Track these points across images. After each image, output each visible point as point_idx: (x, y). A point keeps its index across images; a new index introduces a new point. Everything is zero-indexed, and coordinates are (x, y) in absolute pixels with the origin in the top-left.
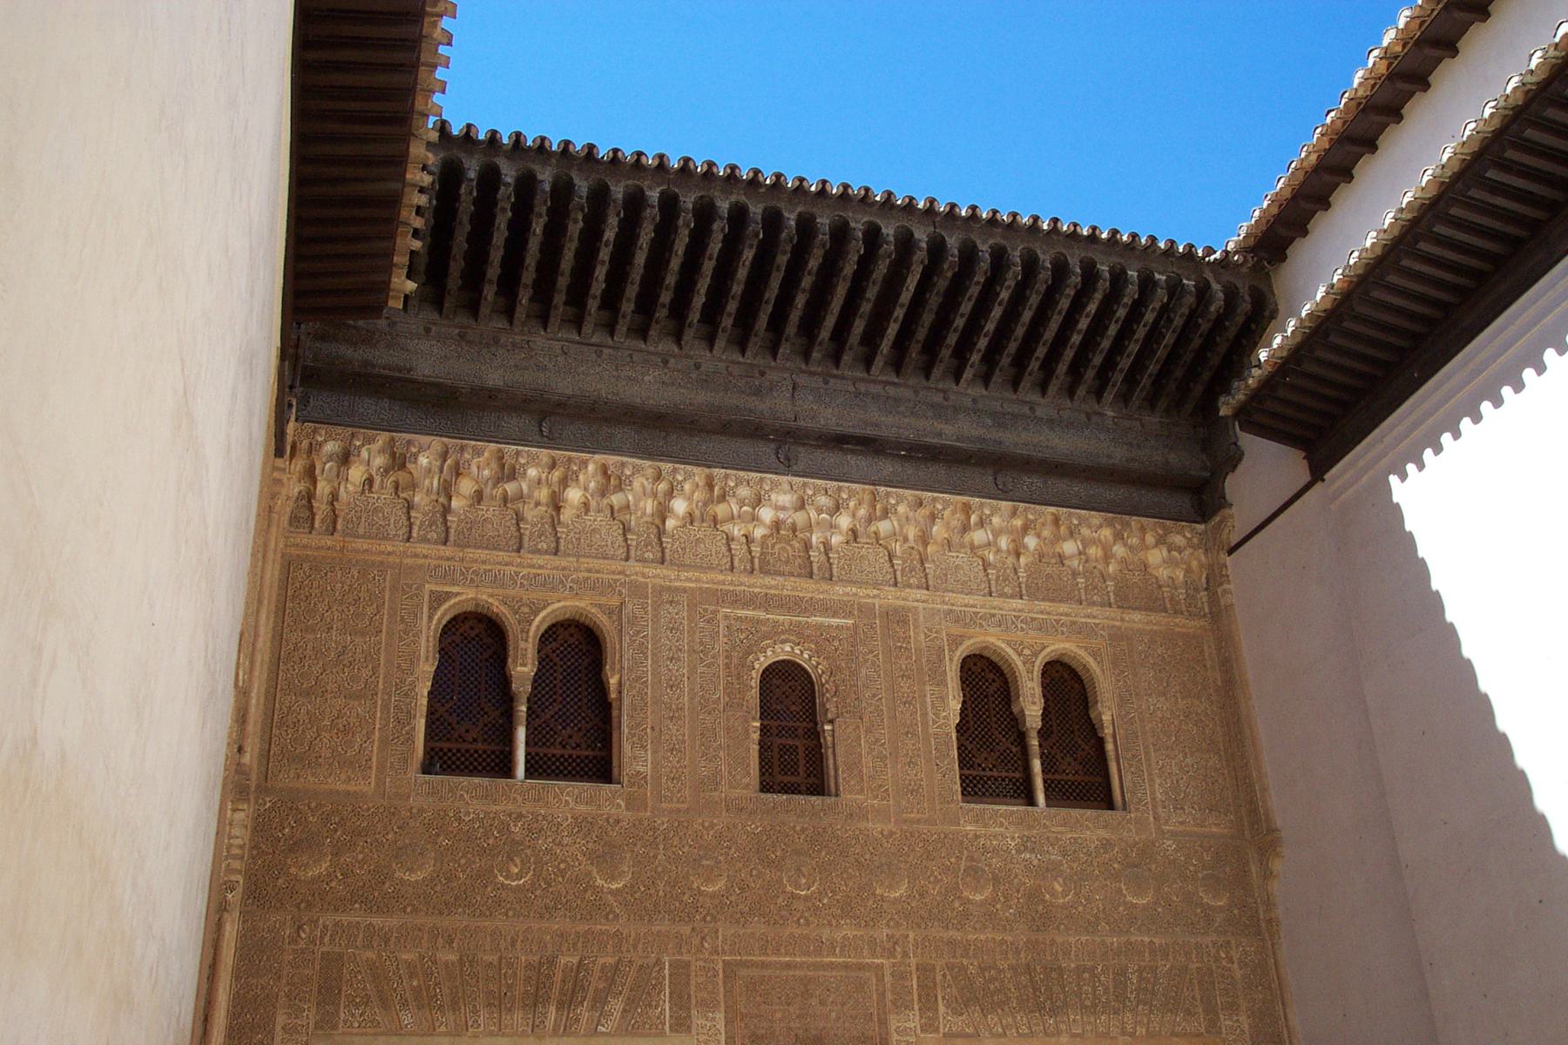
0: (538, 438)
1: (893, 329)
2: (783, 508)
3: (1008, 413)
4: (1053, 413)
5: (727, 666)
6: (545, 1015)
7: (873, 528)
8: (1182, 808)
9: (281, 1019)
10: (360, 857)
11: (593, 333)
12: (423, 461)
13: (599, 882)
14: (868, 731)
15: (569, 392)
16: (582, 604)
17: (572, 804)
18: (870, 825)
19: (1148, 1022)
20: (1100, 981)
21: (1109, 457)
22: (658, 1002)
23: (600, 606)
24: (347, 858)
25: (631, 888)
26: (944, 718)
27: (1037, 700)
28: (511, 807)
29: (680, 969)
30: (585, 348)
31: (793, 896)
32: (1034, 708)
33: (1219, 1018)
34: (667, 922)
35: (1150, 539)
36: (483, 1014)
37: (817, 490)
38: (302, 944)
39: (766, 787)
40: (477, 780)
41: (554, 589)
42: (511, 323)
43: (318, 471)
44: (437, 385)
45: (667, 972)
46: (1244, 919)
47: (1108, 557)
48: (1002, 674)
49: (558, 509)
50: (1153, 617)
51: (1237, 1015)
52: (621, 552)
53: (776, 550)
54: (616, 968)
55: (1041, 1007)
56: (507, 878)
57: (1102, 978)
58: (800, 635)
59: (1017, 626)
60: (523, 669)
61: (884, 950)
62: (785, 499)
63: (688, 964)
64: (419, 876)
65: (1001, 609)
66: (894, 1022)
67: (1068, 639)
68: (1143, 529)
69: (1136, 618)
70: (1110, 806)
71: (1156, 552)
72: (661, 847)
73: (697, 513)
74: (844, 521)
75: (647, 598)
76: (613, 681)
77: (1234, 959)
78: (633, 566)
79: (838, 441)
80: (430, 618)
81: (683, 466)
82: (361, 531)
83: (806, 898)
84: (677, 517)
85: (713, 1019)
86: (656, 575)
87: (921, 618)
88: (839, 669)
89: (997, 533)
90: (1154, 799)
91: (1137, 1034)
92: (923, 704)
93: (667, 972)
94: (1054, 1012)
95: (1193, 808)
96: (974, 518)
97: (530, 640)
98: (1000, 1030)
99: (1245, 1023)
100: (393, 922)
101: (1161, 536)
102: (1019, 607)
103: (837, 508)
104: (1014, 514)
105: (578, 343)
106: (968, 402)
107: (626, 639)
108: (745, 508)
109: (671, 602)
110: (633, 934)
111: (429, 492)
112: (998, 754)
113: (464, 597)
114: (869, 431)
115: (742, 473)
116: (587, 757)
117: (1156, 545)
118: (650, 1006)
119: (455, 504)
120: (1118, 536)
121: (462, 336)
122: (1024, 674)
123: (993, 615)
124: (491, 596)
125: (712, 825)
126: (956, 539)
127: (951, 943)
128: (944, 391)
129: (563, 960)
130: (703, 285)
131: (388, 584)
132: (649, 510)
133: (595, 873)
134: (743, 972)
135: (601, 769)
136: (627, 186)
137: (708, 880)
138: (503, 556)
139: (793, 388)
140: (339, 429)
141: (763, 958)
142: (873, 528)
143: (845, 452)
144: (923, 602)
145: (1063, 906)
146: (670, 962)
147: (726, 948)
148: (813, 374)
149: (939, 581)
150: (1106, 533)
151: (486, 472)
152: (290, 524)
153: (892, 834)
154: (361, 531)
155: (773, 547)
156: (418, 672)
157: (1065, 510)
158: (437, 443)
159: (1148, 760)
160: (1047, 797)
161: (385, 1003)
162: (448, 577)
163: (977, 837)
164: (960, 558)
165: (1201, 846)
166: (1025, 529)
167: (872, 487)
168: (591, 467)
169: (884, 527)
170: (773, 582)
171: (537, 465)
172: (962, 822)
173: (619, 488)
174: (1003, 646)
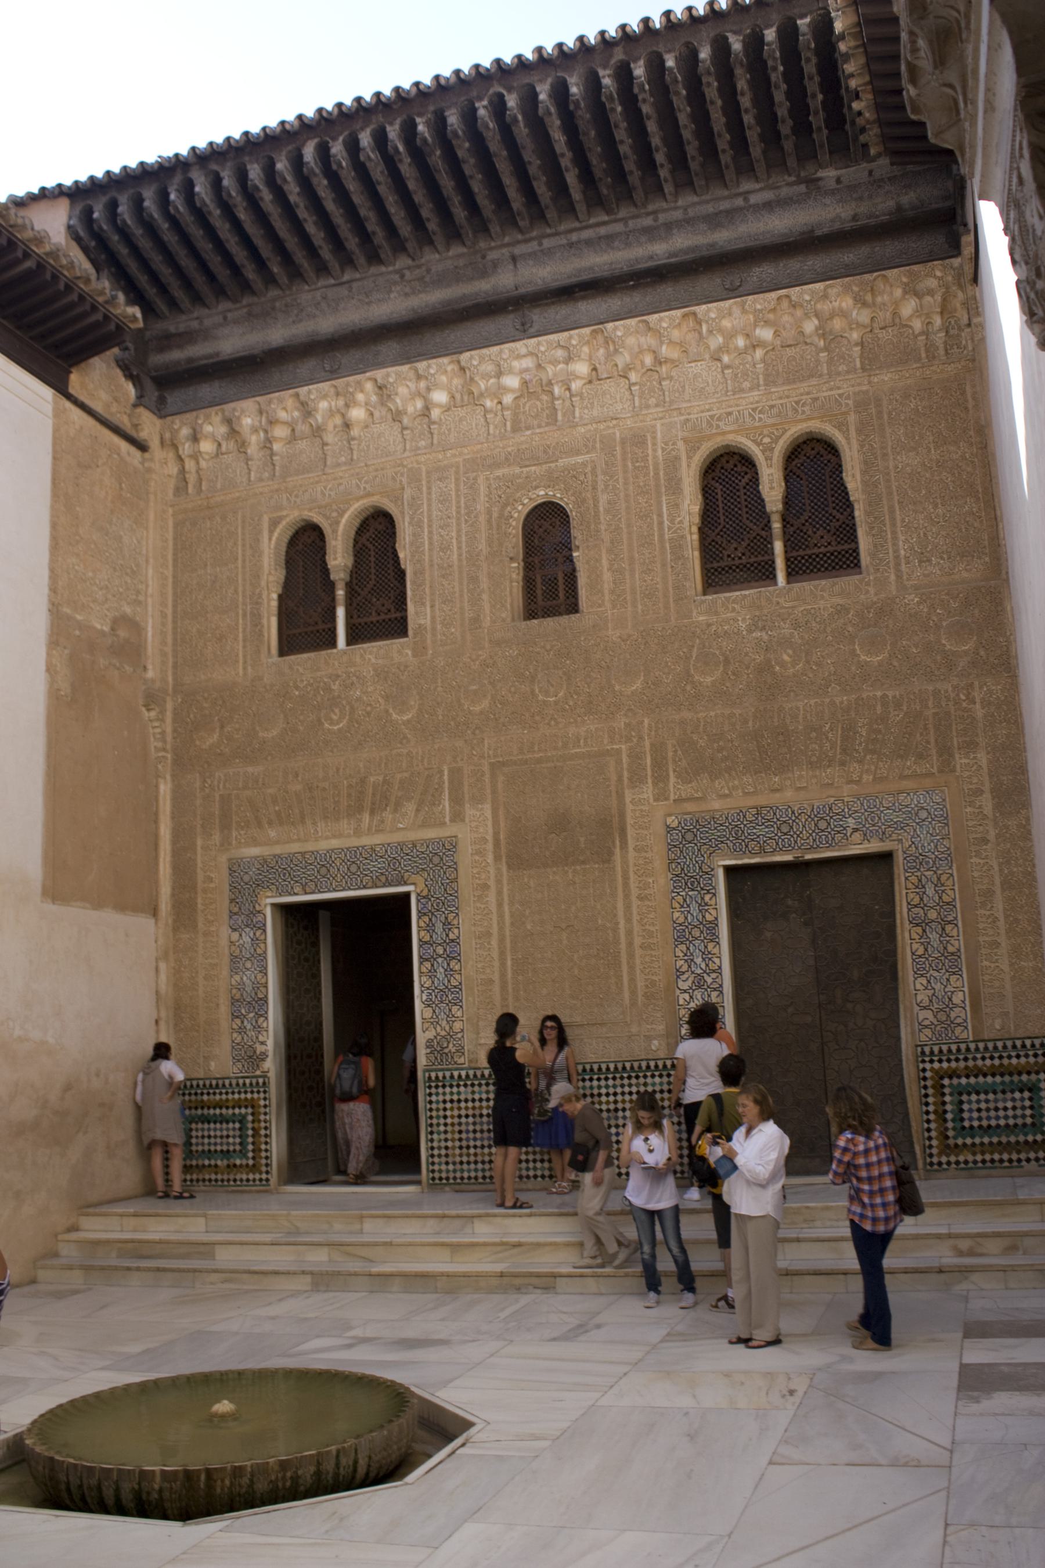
0: (323, 374)
1: (571, 178)
2: (527, 370)
3: (721, 212)
4: (768, 195)
5: (489, 521)
6: (360, 820)
8: (929, 561)
9: (199, 842)
10: (237, 726)
11: (343, 271)
13: (394, 716)
14: (609, 551)
15: (331, 330)
17: (373, 660)
18: (610, 632)
19: (876, 768)
20: (827, 738)
21: (833, 221)
22: (440, 803)
24: (228, 729)
26: (681, 522)
27: (775, 485)
29: (456, 774)
31: (544, 701)
32: (774, 493)
33: (952, 755)
34: (446, 739)
35: (898, 292)
36: (321, 825)
38: (207, 791)
40: (305, 656)
43: (181, 452)
45: (446, 777)
46: (991, 659)
48: (754, 466)
51: (974, 753)
52: (400, 447)
53: (527, 408)
56: (331, 724)
57: (830, 735)
58: (551, 480)
59: (754, 419)
61: (621, 737)
65: (737, 405)
66: (628, 795)
69: (886, 378)
72: (439, 681)
73: (458, 396)
74: (582, 368)
75: (420, 481)
76: (401, 555)
77: (978, 700)
80: (270, 539)
81: (434, 361)
82: (219, 486)
83: (556, 703)
84: (439, 406)
85: (482, 809)
87: (659, 435)
88: (584, 501)
89: (730, 336)
90: (897, 558)
91: (864, 781)
92: (660, 515)
93: (446, 777)
95: (942, 558)
97: (339, 538)
98: (727, 792)
99: (983, 758)
101: (906, 284)
102: (756, 399)
105: (334, 285)
107: (407, 519)
108: (492, 381)
109: (440, 479)
110: (420, 753)
112: (747, 542)
113: (292, 517)
114: (585, 277)
115: (485, 351)
116: (396, 619)
117: (903, 298)
118: (434, 804)
119: (276, 447)
121: (250, 314)
123: (730, 414)
124: (310, 510)
128: (654, 212)
131: (240, 521)
133: (391, 711)
134: (506, 770)
135: (398, 627)
136: (290, 152)
139: (514, 259)
140: (188, 415)
141: (520, 757)
143: (576, 300)
144: (661, 418)
146: (451, 771)
147: (491, 752)
148: (526, 241)
149: (677, 395)
152: (175, 495)
153: (629, 636)
154: (219, 486)
155: (524, 405)
156: (263, 583)
157: (798, 288)
159: (893, 519)
161: (260, 825)
163: (709, 625)
165: (947, 594)
167: (600, 326)
170: (523, 439)
171: (325, 397)
172: (694, 614)
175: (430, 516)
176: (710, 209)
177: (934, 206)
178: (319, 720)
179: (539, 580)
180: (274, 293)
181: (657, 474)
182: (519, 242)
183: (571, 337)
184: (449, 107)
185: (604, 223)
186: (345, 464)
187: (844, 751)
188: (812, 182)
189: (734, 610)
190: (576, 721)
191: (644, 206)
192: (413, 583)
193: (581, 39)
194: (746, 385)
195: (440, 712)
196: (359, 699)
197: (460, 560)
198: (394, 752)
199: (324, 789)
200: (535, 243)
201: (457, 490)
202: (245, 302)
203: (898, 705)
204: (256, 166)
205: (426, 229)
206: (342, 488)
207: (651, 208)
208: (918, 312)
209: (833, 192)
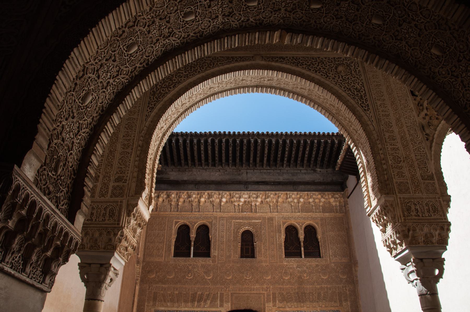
1: (265, 159)
2: (246, 198)
5: (234, 232)
6: (194, 304)
7: (266, 200)
9: (146, 304)
12: (173, 196)
13: (206, 277)
14: (264, 244)
15: (200, 179)
16: (204, 222)
21: (319, 179)
23: (208, 222)
24: (158, 274)
25: (213, 278)
28: (189, 263)
29: (222, 295)
30: (203, 170)
33: (342, 302)
35: (330, 196)
37: (253, 194)
39: (242, 256)
41: (198, 219)
42: (188, 166)
44: (175, 181)
47: (320, 202)
49: (199, 203)
50: (331, 214)
52: (212, 210)
54: (209, 295)
55: (300, 302)
58: (250, 225)
60: (193, 235)
62: (246, 196)
63: (223, 294)
64: (170, 277)
66: (266, 305)
67: (310, 221)
68: (328, 194)
70: (320, 257)
71: (331, 199)
73: (228, 201)
74: (259, 200)
76: (210, 237)
78: (215, 213)
79: (258, 183)
80: (175, 227)
82: (162, 210)
83: (249, 279)
84: (224, 202)
86: (219, 214)
88: (258, 231)
89: (293, 199)
90: (329, 255)
92: (276, 238)
94: (303, 302)
96: (288, 196)
99: (349, 303)
100: (167, 286)
103: (257, 197)
104: (297, 194)
106: (286, 171)
111: (175, 201)
114: (263, 180)
115: (237, 192)
119: (180, 204)
120: (322, 197)
122: (300, 229)
125: (229, 265)
126: (285, 201)
127: (280, 288)
128: (280, 169)
129: (198, 293)
130: (224, 155)
132: (218, 201)
134: (235, 295)
135: (208, 255)
137: (228, 277)
138: (189, 213)
139: (247, 173)
142: (266, 200)
143: (260, 185)
145: (307, 280)
150: (319, 196)
151: (186, 197)
153: (268, 265)
154: (162, 210)
156: (172, 237)
158: (175, 192)
160: (305, 256)
161: (165, 301)
162: (178, 218)
163: (287, 265)
164: (286, 205)
166: (300, 198)
168: (206, 194)
169: (268, 200)
173: (211, 198)
174: (295, 223)
175: (219, 228)
176: (292, 171)
177: (340, 181)
178: (185, 276)
179: (244, 249)
180: (186, 167)
181: (275, 228)
182: (248, 169)
183: (258, 193)
184: (245, 139)
185: (269, 169)
186: (197, 212)
187: (318, 299)
188: (315, 171)
189: (293, 262)
190: (254, 285)
191: (278, 167)
192: (213, 244)
193: (277, 132)
194: (297, 211)
195: (218, 278)
196: (196, 272)
197: (226, 240)
198: (205, 287)
199: (185, 294)
200: (252, 170)
201: (226, 223)
202: (178, 167)
203: (330, 289)
204: (196, 140)
205: (229, 162)
206: (196, 217)
207: (279, 168)
208: (335, 201)
209: (319, 174)
